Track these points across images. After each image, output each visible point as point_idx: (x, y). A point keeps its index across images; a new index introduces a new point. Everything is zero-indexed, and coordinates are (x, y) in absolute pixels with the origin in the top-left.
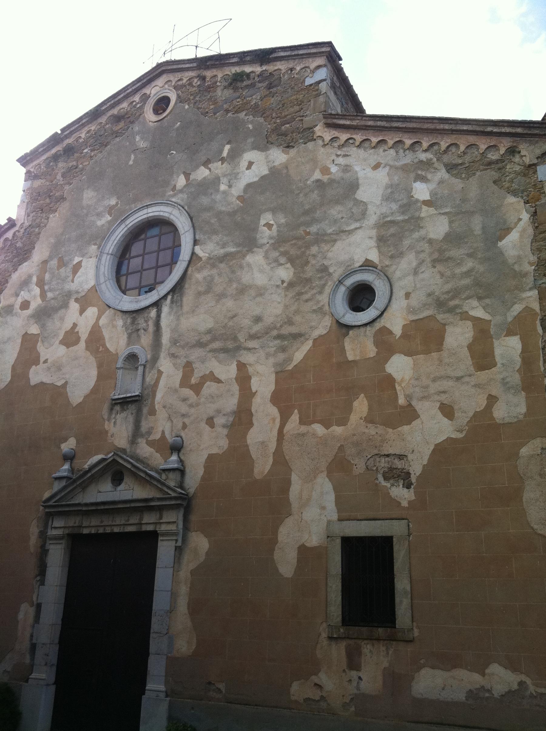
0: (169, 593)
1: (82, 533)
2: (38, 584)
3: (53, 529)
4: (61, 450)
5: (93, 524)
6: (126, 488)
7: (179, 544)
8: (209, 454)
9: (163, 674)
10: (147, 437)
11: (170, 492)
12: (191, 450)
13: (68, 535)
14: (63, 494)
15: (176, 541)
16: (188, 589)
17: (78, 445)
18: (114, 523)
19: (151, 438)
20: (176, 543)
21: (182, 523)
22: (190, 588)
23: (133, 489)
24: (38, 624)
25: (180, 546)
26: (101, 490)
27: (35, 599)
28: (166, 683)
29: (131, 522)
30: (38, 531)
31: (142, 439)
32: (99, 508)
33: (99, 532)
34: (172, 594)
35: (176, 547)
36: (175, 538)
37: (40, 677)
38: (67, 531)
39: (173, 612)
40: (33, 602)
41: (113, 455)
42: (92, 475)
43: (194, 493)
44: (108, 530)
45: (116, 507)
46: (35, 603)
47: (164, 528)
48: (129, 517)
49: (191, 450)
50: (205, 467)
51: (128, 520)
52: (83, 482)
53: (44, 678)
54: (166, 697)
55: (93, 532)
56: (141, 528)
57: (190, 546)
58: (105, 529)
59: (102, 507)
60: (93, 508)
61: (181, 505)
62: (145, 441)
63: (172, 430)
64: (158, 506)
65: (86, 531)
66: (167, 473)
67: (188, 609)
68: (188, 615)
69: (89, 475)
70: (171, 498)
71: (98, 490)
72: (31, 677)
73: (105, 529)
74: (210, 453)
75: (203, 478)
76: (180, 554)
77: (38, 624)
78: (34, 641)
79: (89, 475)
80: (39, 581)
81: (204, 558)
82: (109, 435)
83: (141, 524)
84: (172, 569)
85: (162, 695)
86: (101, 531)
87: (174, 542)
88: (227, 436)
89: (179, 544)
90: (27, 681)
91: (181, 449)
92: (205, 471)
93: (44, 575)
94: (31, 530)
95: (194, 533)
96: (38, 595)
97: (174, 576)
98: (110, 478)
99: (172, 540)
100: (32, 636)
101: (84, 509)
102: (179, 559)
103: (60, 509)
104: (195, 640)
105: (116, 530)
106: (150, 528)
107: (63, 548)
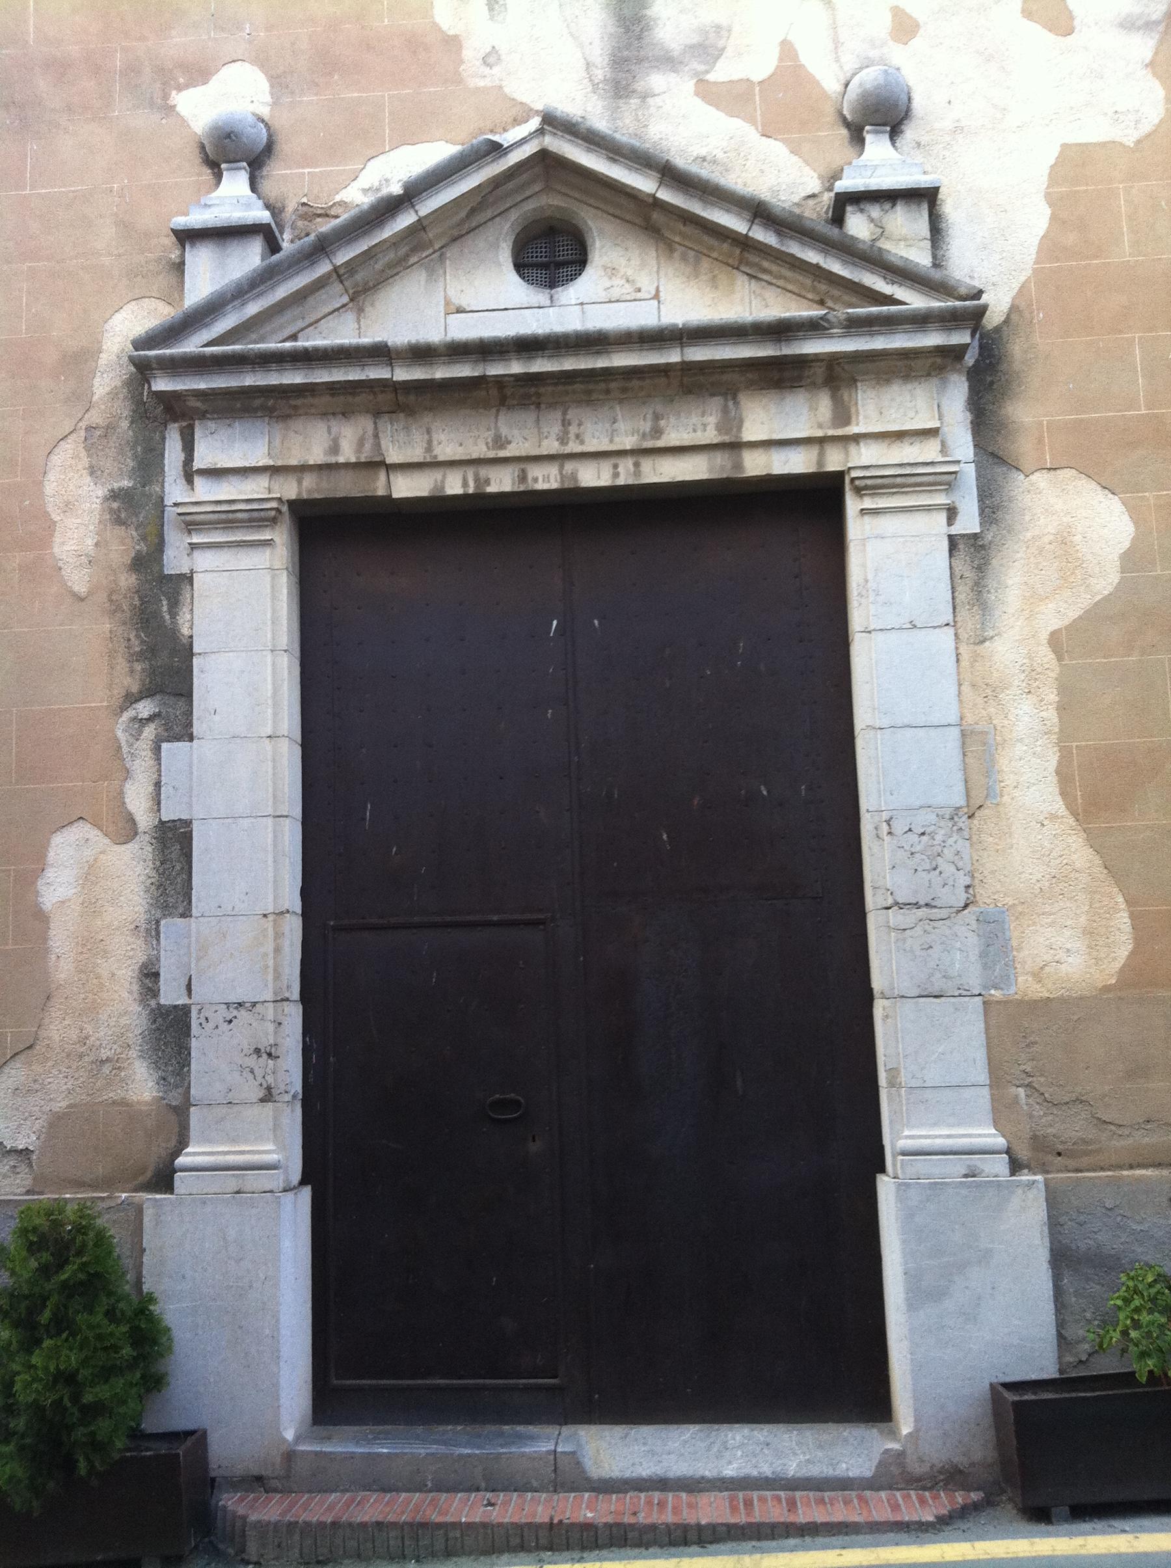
0: (955, 733)
1: (388, 499)
2: (150, 731)
3: (198, 481)
4: (183, 121)
5: (447, 449)
6: (616, 293)
7: (969, 522)
8: (1065, 146)
9: (981, 1075)
10: (701, 68)
11: (899, 292)
12: (958, 129)
13: (296, 506)
14: (253, 308)
15: (952, 513)
16: (1051, 715)
17: (287, 100)
18: (573, 447)
19: (722, 73)
20: (951, 520)
21: (969, 437)
22: (1061, 708)
23: (657, 296)
24: (186, 914)
25: (975, 536)
26: (465, 301)
27: (137, 800)
28: (1001, 1112)
29: (673, 437)
30: (101, 492)
31: (673, 78)
32: (495, 370)
33: (489, 489)
34: (963, 734)
35: (953, 541)
36: (941, 499)
37: (938, 1141)
38: (289, 489)
39: (985, 812)
40: (131, 820)
41: (540, 132)
42: (419, 227)
43: (1014, 308)
44: (546, 479)
45: (601, 363)
46: (145, 820)
47: (867, 456)
48: (657, 417)
49: (958, 129)
50: (1049, 198)
51: (657, 432)
52: (368, 255)
53: (273, 1158)
54: (1012, 1174)
55: (454, 486)
56: (739, 466)
57: (1029, 535)
58: (523, 478)
59: (516, 367)
60: (464, 370)
61: (954, 354)
62: (690, 85)
63: (837, 44)
64: (833, 360)
65: (406, 487)
66: (875, 211)
67: (1064, 794)
68: (1071, 821)
69: (405, 220)
70: (921, 321)
71: (448, 303)
72: (181, 1161)
73: (523, 478)
74: (1071, 139)
75: (1050, 248)
76: (981, 568)
77: (186, 914)
78: (171, 995)
79: (405, 220)
80: (151, 719)
81: (1114, 578)
82: (467, 54)
83: (736, 446)
84: (950, 631)
85: (999, 1166)
86: (502, 482)
87: (942, 517)
88: (1151, 65)
89: (969, 522)
90: (163, 1180)
91: (903, 120)
92: (1054, 218)
93: (184, 692)
94: (50, 488)
95: (1040, 479)
96: (158, 785)
97: (965, 663)
98: (505, 256)
99: (928, 509)
100: (150, 975)
101: (402, 374)
102: (979, 588)
103: (250, 380)
104: (1123, 920)
105: (593, 476)
106: (796, 463)
107: (277, 565)
